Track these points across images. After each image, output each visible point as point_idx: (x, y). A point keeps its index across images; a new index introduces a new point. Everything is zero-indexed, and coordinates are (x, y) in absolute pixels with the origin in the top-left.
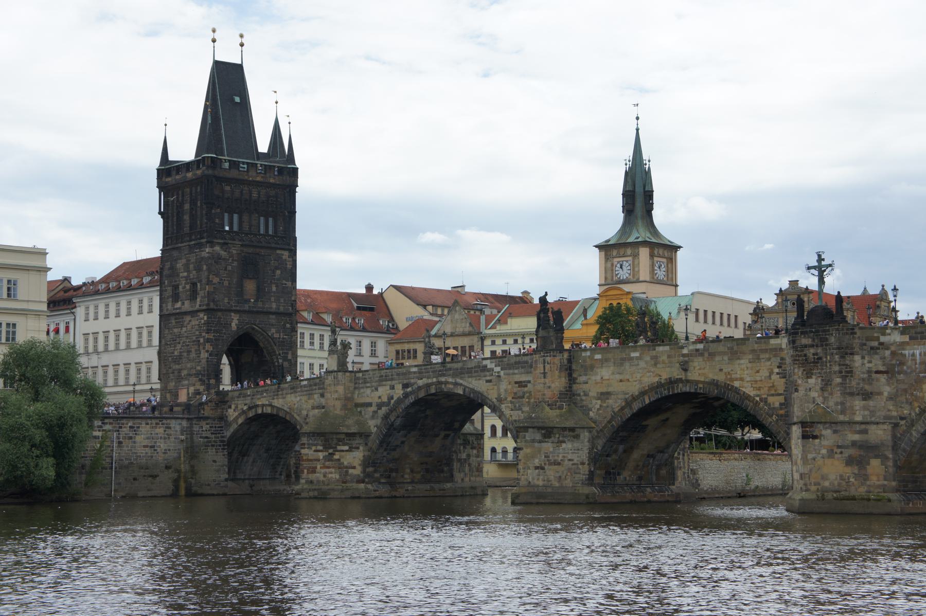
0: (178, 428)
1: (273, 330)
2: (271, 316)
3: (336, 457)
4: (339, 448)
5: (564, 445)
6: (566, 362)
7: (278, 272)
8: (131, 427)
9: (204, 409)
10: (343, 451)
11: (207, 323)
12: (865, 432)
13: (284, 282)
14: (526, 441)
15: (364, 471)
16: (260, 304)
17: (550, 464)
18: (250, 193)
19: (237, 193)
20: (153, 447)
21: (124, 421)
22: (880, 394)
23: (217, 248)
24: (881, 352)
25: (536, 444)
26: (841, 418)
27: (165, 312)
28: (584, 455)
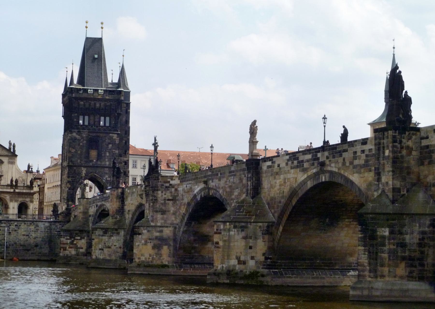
0: (42, 226)
1: (107, 176)
2: (105, 169)
3: (75, 242)
4: (76, 238)
5: (112, 238)
6: (120, 194)
7: (110, 146)
8: (16, 225)
9: (59, 217)
10: (77, 239)
12: (161, 231)
13: (114, 151)
14: (96, 235)
17: (106, 247)
19: (87, 105)
20: (28, 235)
21: (12, 222)
22: (169, 211)
23: (74, 134)
24: (170, 189)
25: (100, 237)
26: (152, 224)
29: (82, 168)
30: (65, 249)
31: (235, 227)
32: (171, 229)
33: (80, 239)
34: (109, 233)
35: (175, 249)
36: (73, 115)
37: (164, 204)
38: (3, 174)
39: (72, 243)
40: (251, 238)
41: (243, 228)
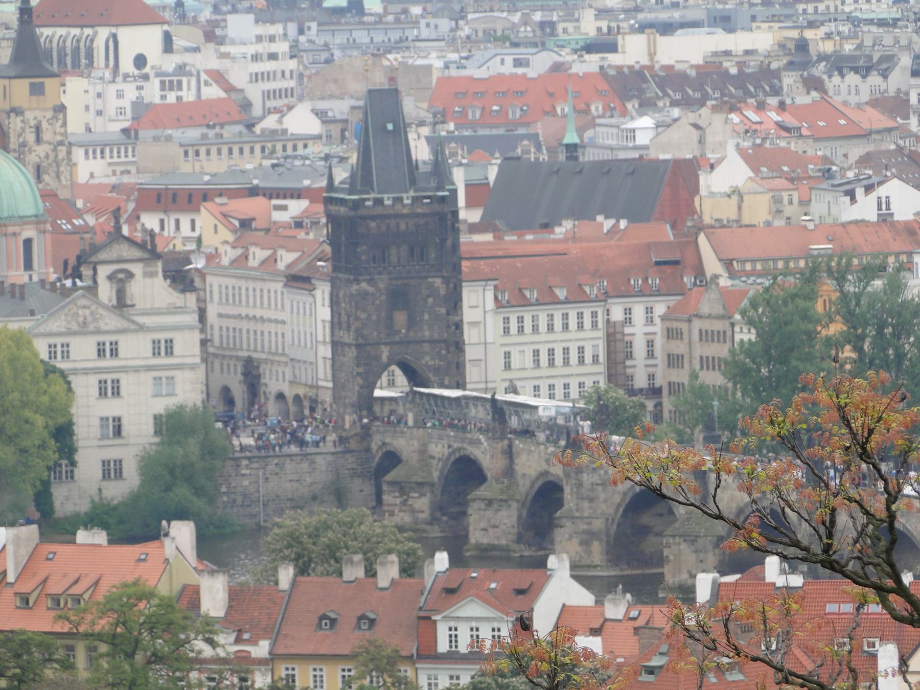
0: (322, 462)
1: (427, 358)
4: (412, 495)
5: (500, 513)
6: (506, 448)
7: (430, 300)
11: (357, 358)
12: (590, 524)
13: (437, 309)
15: (432, 514)
16: (412, 334)
18: (398, 225)
21: (270, 459)
25: (482, 512)
26: (577, 514)
27: (335, 339)
28: (514, 519)
29: (383, 347)
30: (392, 514)
31: (685, 541)
32: (602, 520)
33: (418, 498)
34: (495, 506)
35: (608, 543)
36: (358, 250)
37: (592, 490)
38: (134, 302)
39: (404, 503)
40: (701, 551)
41: (693, 542)
